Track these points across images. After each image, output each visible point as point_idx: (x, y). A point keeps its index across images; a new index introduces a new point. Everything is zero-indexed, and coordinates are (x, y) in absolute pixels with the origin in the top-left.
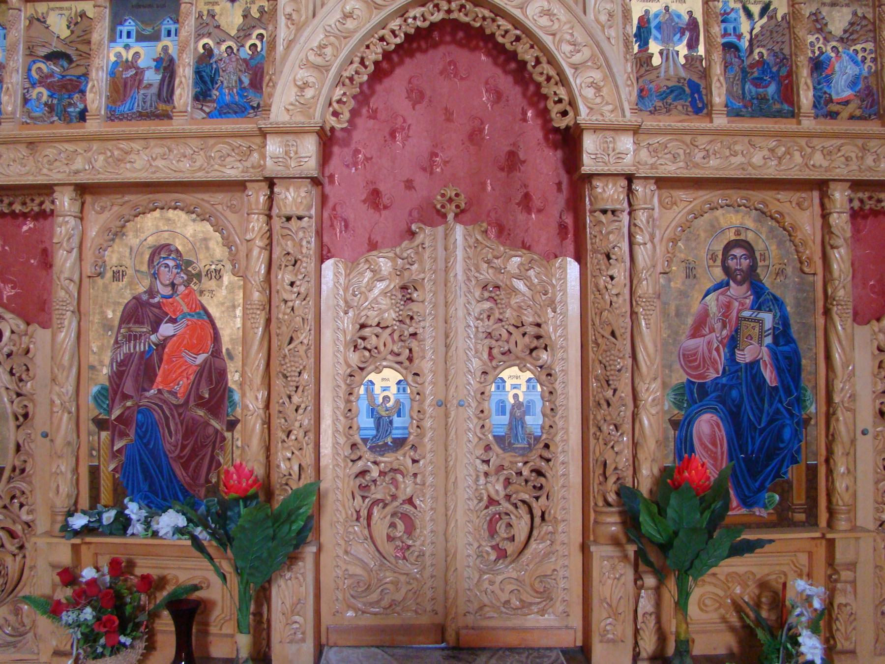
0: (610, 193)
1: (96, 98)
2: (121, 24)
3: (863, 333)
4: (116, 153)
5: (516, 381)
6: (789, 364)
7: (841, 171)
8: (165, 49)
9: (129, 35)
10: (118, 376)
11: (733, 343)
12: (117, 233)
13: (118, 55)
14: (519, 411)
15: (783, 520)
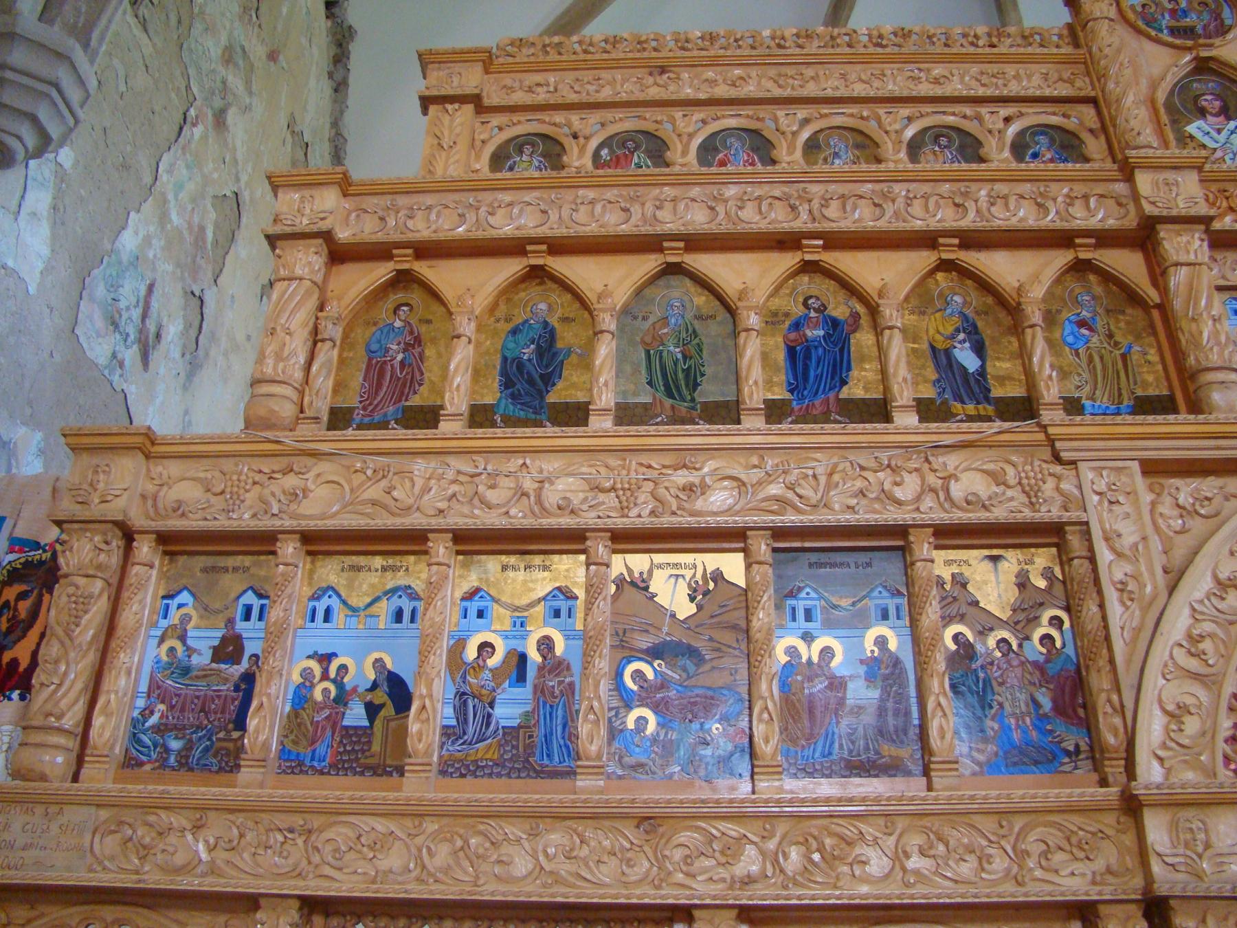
2: (791, 595)
4: (828, 841)
8: (881, 642)
9: (809, 616)
13: (792, 651)
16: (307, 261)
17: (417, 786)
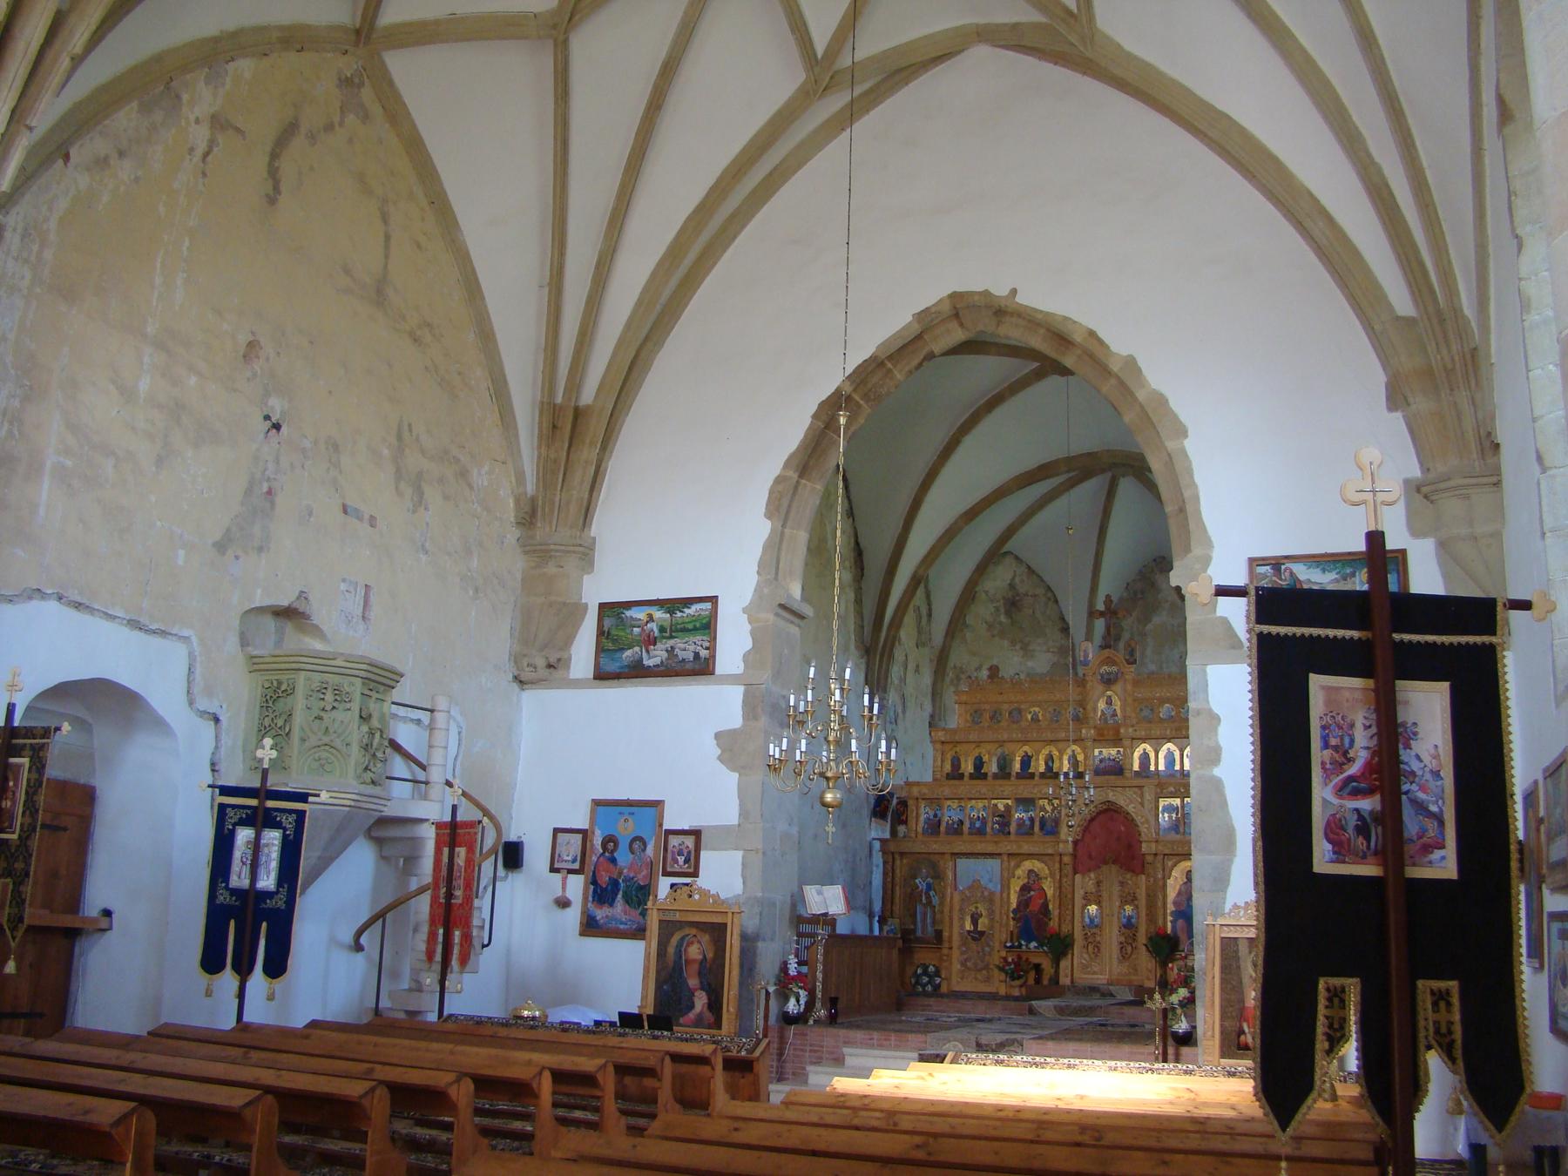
0: (1149, 859)
1: (1013, 828)
5: (1129, 909)
10: (1019, 904)
12: (1017, 866)
14: (1130, 918)
16: (939, 746)
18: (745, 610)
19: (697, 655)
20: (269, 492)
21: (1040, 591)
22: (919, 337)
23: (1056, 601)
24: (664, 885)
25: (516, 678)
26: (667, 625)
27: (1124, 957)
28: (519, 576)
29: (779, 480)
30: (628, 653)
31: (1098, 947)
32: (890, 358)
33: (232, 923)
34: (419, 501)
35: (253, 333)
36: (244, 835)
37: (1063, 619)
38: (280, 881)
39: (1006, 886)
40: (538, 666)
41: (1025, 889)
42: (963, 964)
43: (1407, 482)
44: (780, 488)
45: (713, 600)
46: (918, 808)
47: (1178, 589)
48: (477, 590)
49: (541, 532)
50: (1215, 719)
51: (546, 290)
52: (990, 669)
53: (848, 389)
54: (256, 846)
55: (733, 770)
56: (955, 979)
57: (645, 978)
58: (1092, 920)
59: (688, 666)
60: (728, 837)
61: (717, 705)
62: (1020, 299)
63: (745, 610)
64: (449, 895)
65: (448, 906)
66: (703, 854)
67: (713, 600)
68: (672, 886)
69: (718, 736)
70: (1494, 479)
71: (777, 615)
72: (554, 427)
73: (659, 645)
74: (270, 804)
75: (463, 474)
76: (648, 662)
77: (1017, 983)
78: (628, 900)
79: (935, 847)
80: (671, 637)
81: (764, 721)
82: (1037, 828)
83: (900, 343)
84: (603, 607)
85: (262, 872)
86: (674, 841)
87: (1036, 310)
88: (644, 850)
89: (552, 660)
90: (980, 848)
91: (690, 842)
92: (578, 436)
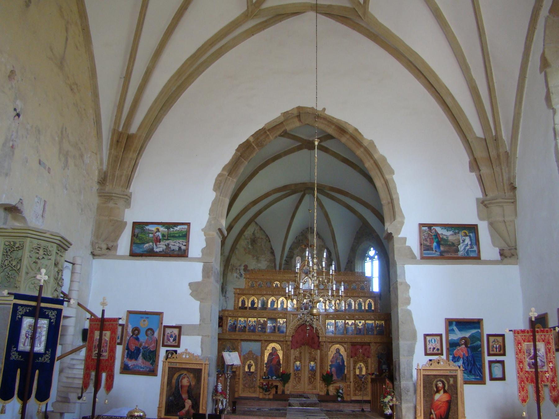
0: (322, 343)
3: (352, 359)
5: (312, 363)
6: (343, 362)
7: (349, 341)
11: (337, 360)
14: (313, 367)
15: (342, 380)
16: (237, 295)
17: (247, 333)
18: (202, 230)
19: (180, 248)
20: (12, 147)
21: (264, 237)
22: (282, 123)
23: (270, 241)
24: (163, 351)
25: (91, 252)
26: (166, 234)
27: (310, 382)
28: (96, 206)
29: (220, 175)
30: (147, 245)
31: (300, 378)
32: (269, 130)
33: (19, 371)
34: (66, 165)
35: (13, 67)
36: (27, 322)
37: (272, 248)
38: (47, 348)
39: (263, 354)
40: (103, 248)
41: (270, 354)
42: (244, 385)
43: (477, 199)
44: (220, 179)
45: (188, 224)
46: (227, 321)
47: (391, 234)
48: (82, 210)
49: (108, 188)
50: (408, 287)
51: (123, 80)
52: (244, 266)
53: (252, 140)
54: (35, 328)
55: (197, 300)
56: (240, 392)
57: (161, 394)
58: (297, 368)
59: (176, 253)
60: (193, 330)
61: (190, 271)
62: (328, 112)
63: (202, 230)
64: (99, 355)
65: (99, 360)
66: (182, 337)
67: (188, 224)
68: (167, 351)
69: (190, 284)
70: (513, 201)
71: (217, 233)
72: (118, 142)
73: (162, 243)
74: (43, 305)
75: (82, 156)
76: (155, 250)
77: (267, 393)
78: (144, 357)
79: (233, 337)
80: (168, 239)
81: (212, 279)
82: (277, 330)
83: (275, 124)
84: (134, 223)
85: (37, 342)
86: (168, 331)
87: (334, 118)
88: (153, 335)
89: (110, 246)
90: (253, 338)
91: (176, 331)
92: (127, 146)
